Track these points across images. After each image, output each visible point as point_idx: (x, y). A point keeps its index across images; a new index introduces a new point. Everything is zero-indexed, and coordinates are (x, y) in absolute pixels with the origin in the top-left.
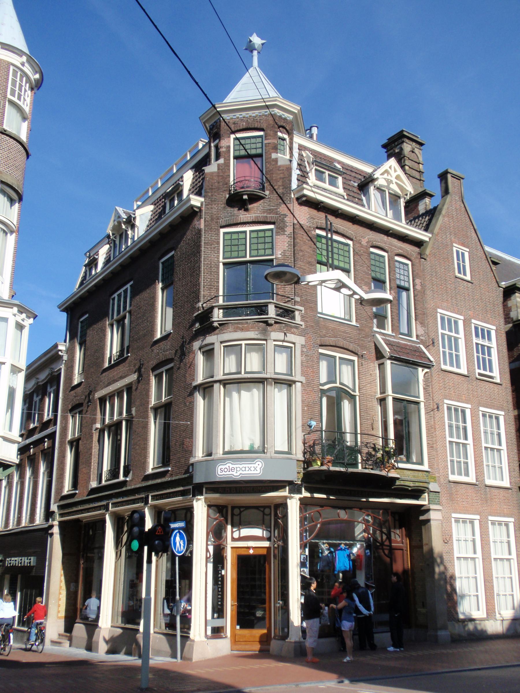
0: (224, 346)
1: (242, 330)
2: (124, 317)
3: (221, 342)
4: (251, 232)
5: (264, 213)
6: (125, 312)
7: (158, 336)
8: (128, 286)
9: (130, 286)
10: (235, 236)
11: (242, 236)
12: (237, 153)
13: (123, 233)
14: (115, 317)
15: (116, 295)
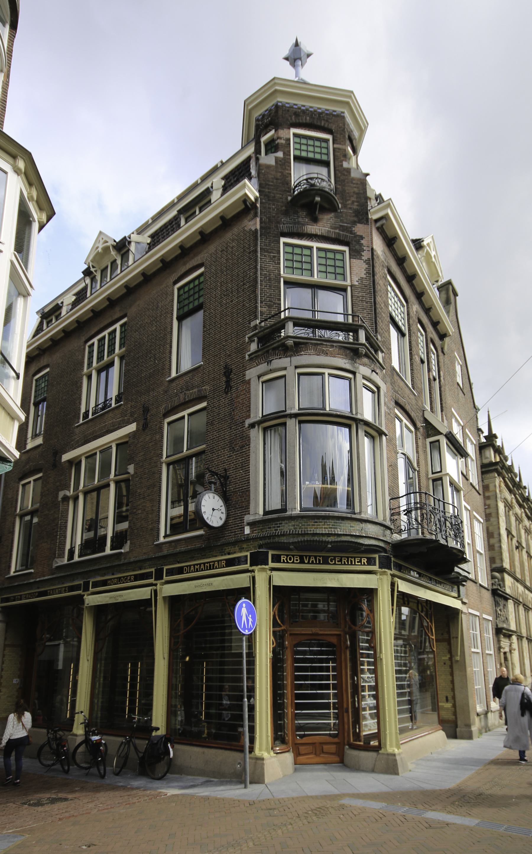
0: (300, 374)
1: (326, 354)
2: (111, 364)
3: (296, 367)
4: (319, 249)
5: (335, 228)
6: (110, 357)
7: (174, 374)
8: (117, 326)
9: (121, 326)
10: (297, 251)
11: (306, 252)
12: (298, 153)
13: (107, 267)
14: (95, 364)
15: (95, 340)
